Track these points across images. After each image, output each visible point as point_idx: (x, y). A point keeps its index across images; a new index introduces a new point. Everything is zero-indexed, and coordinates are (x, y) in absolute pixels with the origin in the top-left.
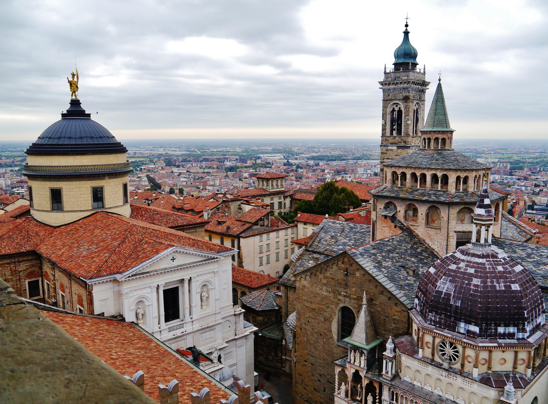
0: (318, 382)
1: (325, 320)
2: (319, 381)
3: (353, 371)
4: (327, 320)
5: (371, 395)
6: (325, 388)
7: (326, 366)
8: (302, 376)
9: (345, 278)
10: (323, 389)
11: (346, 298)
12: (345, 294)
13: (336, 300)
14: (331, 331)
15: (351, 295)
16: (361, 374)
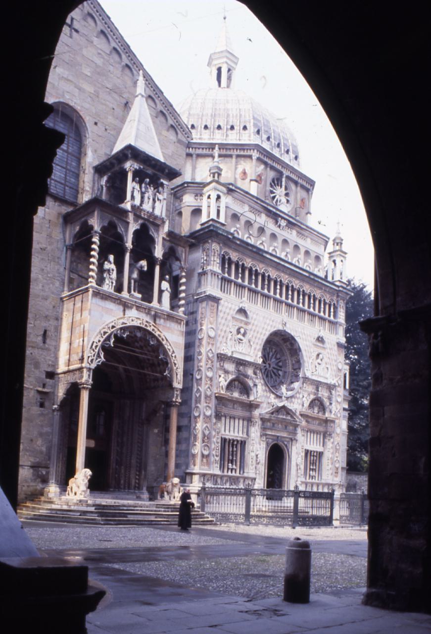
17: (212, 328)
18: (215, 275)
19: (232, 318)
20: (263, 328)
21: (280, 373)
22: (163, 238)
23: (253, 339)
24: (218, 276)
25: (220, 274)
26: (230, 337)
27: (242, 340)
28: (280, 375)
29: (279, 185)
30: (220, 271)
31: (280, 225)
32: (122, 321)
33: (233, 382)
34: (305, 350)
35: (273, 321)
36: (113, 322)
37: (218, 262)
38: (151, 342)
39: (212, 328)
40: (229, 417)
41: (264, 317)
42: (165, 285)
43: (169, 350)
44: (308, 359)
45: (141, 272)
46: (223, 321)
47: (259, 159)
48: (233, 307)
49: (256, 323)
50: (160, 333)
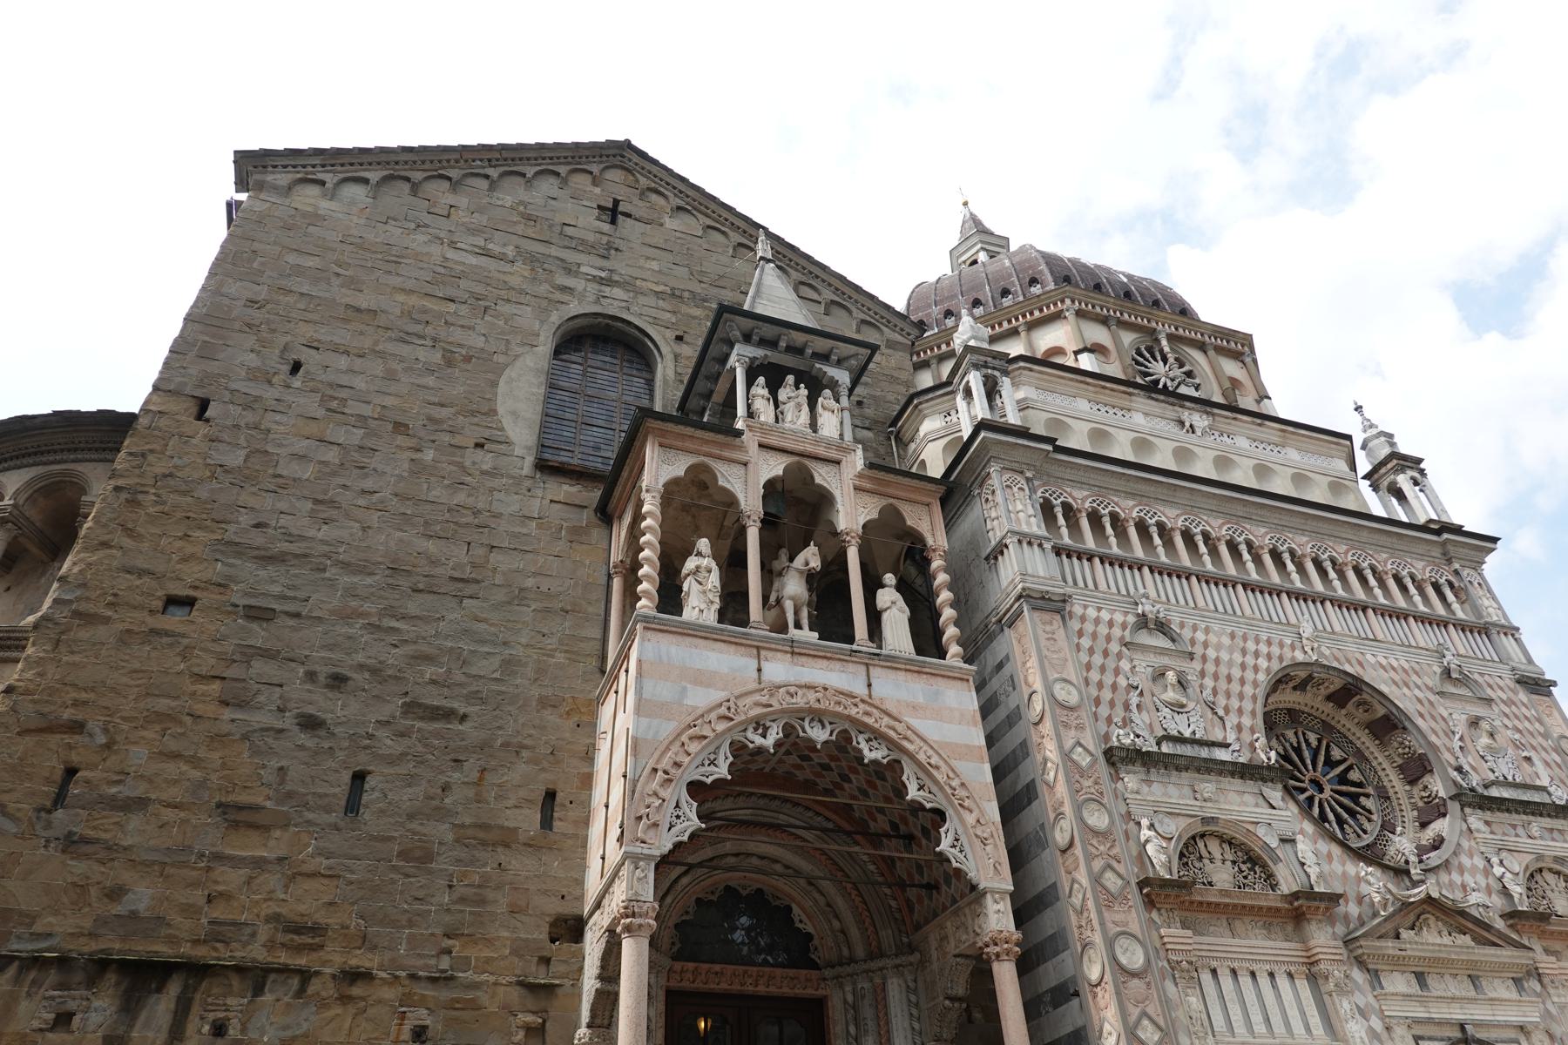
0: (304, 738)
1: (449, 363)
2: (310, 724)
3: (774, 467)
4: (468, 359)
5: (899, 588)
6: (359, 777)
7: (413, 606)
8: (77, 727)
9: (606, 227)
10: (340, 787)
11: (603, 288)
12: (603, 275)
13: (544, 288)
14: (493, 412)
15: (638, 283)
16: (823, 476)
17: (1065, 680)
18: (1030, 543)
19: (1124, 649)
20: (1243, 666)
21: (1369, 803)
22: (856, 488)
23: (1221, 701)
24: (1040, 545)
25: (1046, 539)
26: (1134, 700)
27: (1183, 706)
28: (1370, 812)
29: (1159, 358)
30: (1043, 532)
31: (1191, 426)
32: (757, 697)
33: (1201, 844)
34: (1421, 715)
35: (1269, 643)
36: (721, 705)
37: (1031, 511)
38: (866, 752)
39: (1065, 680)
40: (1228, 972)
41: (1233, 636)
42: (888, 597)
43: (937, 768)
44: (1447, 741)
45: (811, 578)
46: (1098, 659)
47: (1080, 314)
48: (1119, 618)
49: (1211, 653)
50: (892, 723)
